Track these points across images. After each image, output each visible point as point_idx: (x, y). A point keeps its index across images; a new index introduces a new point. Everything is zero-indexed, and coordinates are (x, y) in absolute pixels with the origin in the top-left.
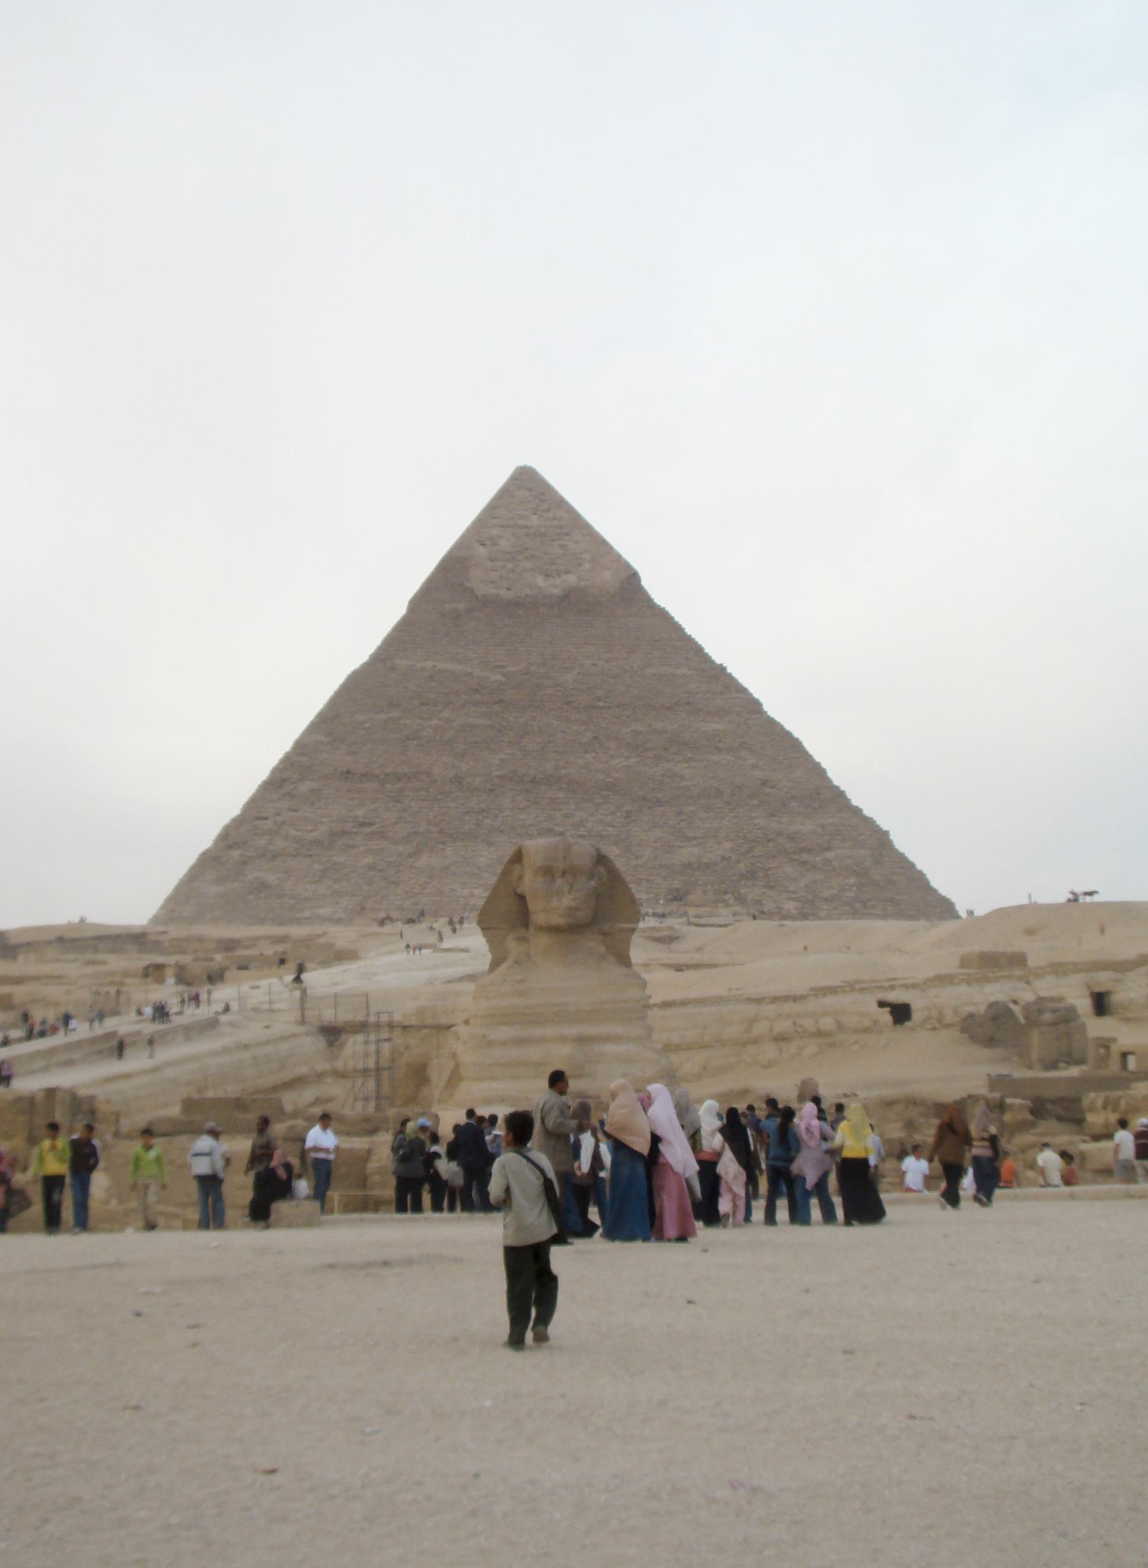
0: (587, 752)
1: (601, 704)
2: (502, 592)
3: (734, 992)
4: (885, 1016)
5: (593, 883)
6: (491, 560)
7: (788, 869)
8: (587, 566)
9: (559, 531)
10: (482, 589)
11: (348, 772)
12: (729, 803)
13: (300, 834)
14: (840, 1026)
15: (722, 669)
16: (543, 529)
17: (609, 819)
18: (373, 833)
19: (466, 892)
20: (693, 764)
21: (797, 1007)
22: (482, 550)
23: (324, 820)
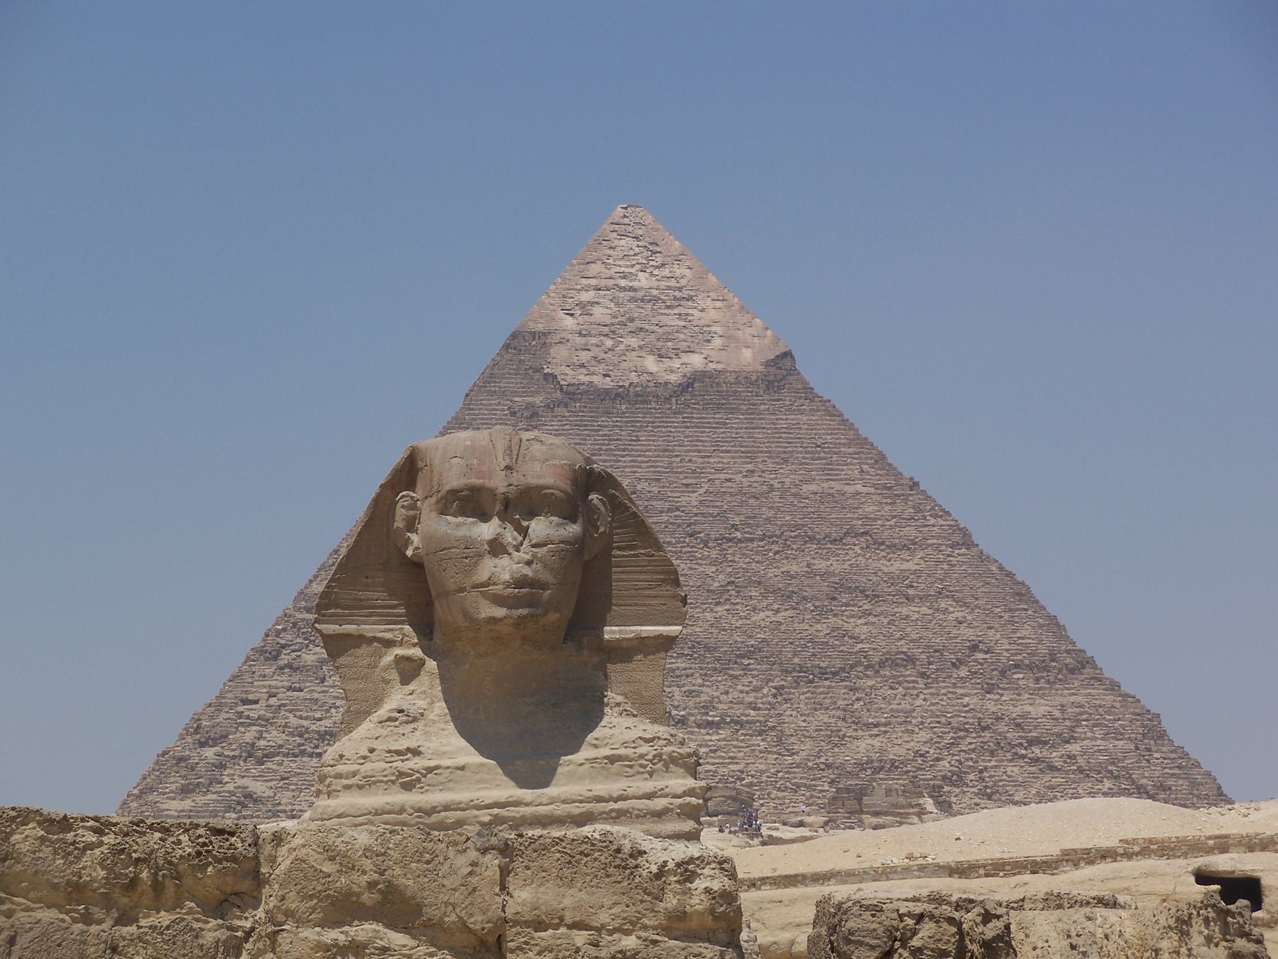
0: (718, 604)
1: (738, 535)
2: (597, 380)
3: (921, 861)
5: (574, 529)
6: (580, 334)
8: (718, 342)
9: (677, 294)
10: (568, 376)
12: (923, 675)
13: (305, 723)
16: (655, 292)
17: (750, 698)
20: (874, 620)
22: (569, 322)
23: (339, 703)
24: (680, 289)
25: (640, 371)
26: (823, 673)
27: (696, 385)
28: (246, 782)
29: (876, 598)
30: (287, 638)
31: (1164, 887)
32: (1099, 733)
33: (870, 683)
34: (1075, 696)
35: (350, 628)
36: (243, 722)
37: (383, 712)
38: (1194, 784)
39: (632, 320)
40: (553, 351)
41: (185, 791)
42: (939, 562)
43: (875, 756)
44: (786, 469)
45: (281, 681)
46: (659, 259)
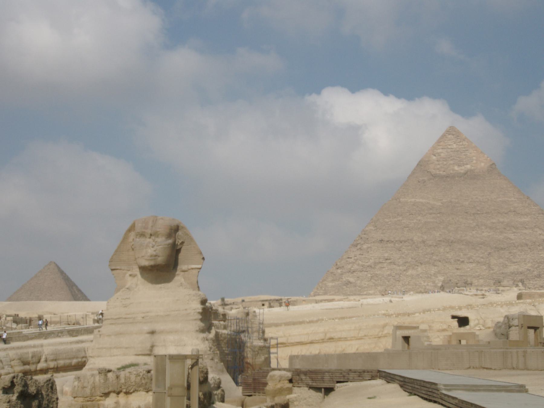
2: (441, 172)
4: (455, 323)
5: (170, 241)
6: (438, 161)
8: (474, 162)
15: (528, 198)
17: (481, 256)
18: (391, 263)
22: (434, 158)
24: (464, 148)
25: (453, 170)
26: (502, 249)
27: (469, 173)
28: (348, 278)
30: (360, 241)
33: (515, 251)
35: (118, 267)
39: (451, 157)
41: (333, 281)
45: (359, 252)
46: (459, 140)
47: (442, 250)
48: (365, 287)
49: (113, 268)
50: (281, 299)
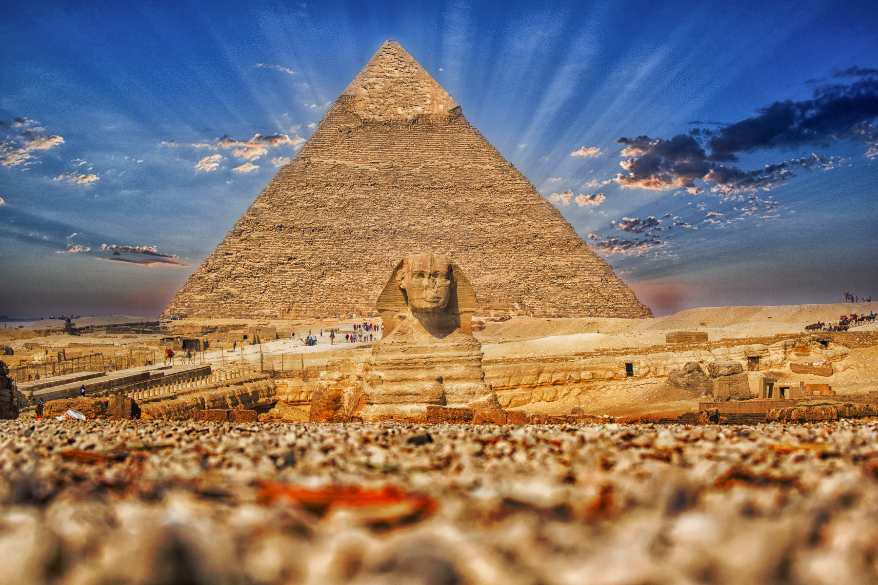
2: (376, 117)
5: (449, 282)
7: (550, 288)
8: (429, 101)
10: (364, 115)
11: (282, 226)
14: (594, 377)
18: (296, 264)
19: (353, 301)
21: (566, 365)
24: (413, 78)
25: (397, 114)
28: (228, 288)
29: (495, 214)
30: (244, 227)
31: (608, 366)
32: (587, 273)
34: (578, 257)
36: (226, 263)
37: (395, 331)
38: (625, 295)
39: (392, 91)
40: (358, 104)
41: (202, 291)
42: (521, 199)
43: (493, 282)
44: (458, 158)
45: (243, 245)
46: (404, 64)
47: (379, 247)
48: (256, 303)
49: (379, 308)
50: (158, 323)
